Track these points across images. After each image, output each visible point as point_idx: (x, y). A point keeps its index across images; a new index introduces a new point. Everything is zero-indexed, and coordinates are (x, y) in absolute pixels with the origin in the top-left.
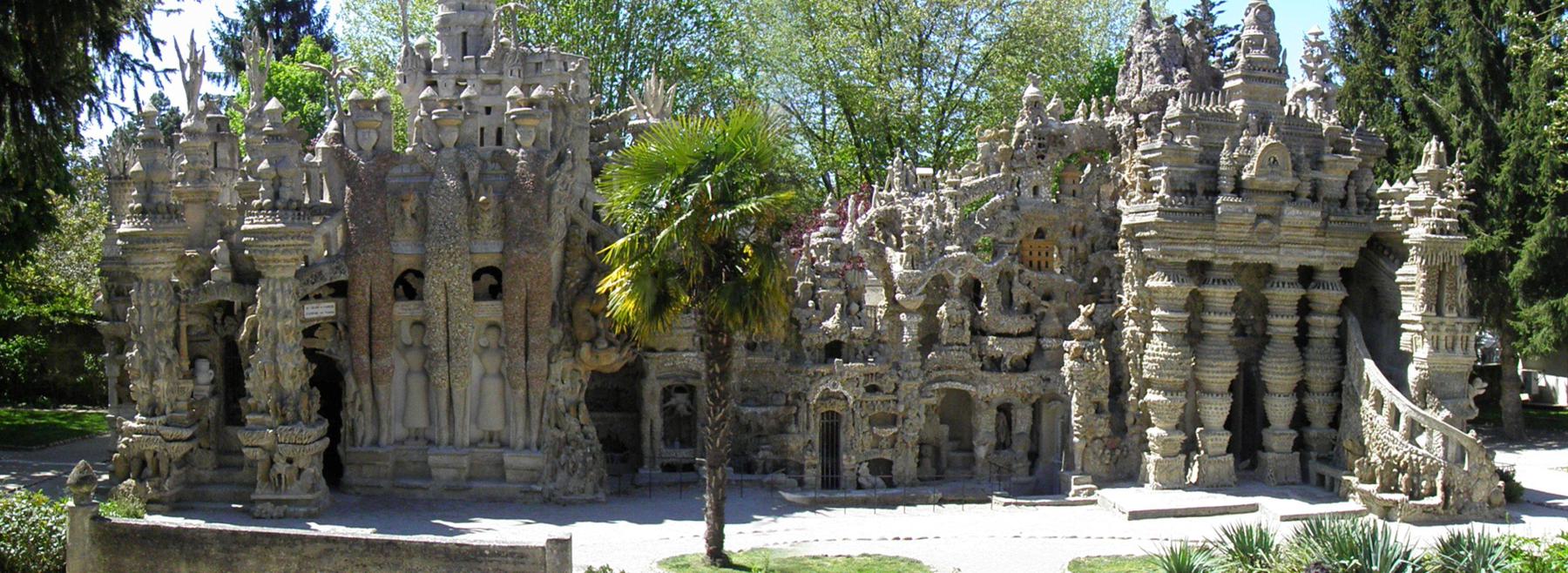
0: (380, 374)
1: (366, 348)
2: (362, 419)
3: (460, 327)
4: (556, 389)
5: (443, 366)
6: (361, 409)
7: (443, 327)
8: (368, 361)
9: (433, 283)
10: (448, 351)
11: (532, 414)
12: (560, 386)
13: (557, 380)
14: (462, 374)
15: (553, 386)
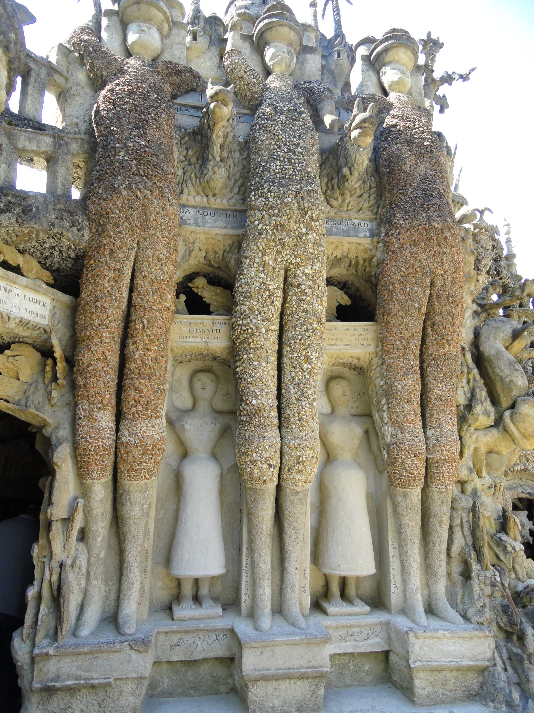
0: (137, 453)
1: (110, 397)
2: (83, 560)
3: (308, 359)
4: (469, 488)
5: (273, 434)
6: (83, 535)
7: (273, 358)
8: (112, 425)
9: (264, 265)
10: (279, 408)
11: (434, 538)
12: (478, 483)
13: (471, 471)
14: (309, 453)
15: (462, 483)
